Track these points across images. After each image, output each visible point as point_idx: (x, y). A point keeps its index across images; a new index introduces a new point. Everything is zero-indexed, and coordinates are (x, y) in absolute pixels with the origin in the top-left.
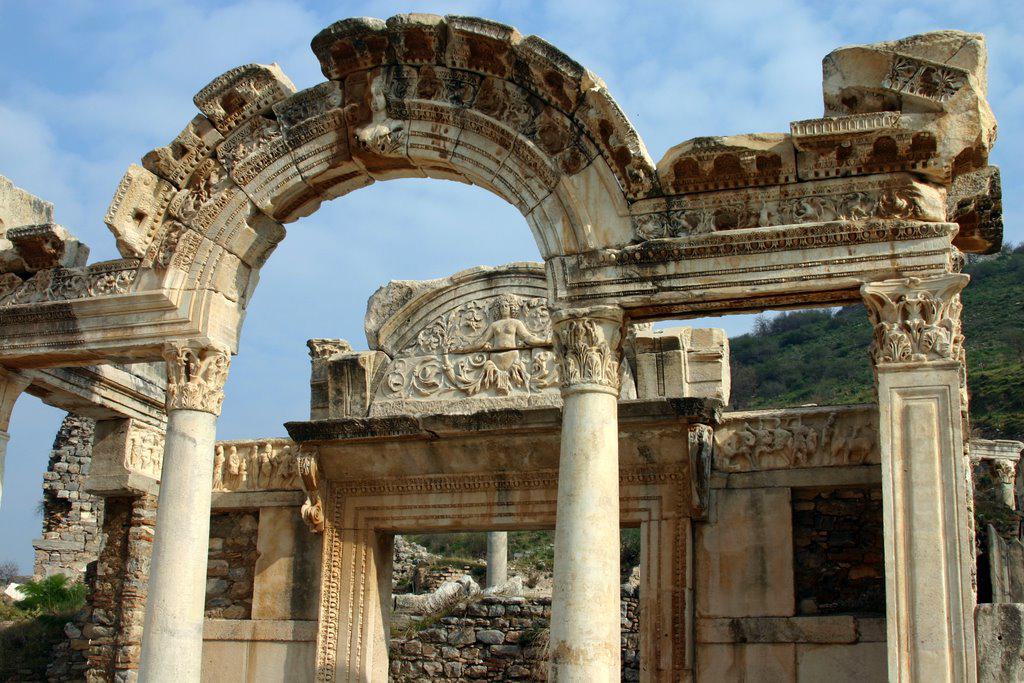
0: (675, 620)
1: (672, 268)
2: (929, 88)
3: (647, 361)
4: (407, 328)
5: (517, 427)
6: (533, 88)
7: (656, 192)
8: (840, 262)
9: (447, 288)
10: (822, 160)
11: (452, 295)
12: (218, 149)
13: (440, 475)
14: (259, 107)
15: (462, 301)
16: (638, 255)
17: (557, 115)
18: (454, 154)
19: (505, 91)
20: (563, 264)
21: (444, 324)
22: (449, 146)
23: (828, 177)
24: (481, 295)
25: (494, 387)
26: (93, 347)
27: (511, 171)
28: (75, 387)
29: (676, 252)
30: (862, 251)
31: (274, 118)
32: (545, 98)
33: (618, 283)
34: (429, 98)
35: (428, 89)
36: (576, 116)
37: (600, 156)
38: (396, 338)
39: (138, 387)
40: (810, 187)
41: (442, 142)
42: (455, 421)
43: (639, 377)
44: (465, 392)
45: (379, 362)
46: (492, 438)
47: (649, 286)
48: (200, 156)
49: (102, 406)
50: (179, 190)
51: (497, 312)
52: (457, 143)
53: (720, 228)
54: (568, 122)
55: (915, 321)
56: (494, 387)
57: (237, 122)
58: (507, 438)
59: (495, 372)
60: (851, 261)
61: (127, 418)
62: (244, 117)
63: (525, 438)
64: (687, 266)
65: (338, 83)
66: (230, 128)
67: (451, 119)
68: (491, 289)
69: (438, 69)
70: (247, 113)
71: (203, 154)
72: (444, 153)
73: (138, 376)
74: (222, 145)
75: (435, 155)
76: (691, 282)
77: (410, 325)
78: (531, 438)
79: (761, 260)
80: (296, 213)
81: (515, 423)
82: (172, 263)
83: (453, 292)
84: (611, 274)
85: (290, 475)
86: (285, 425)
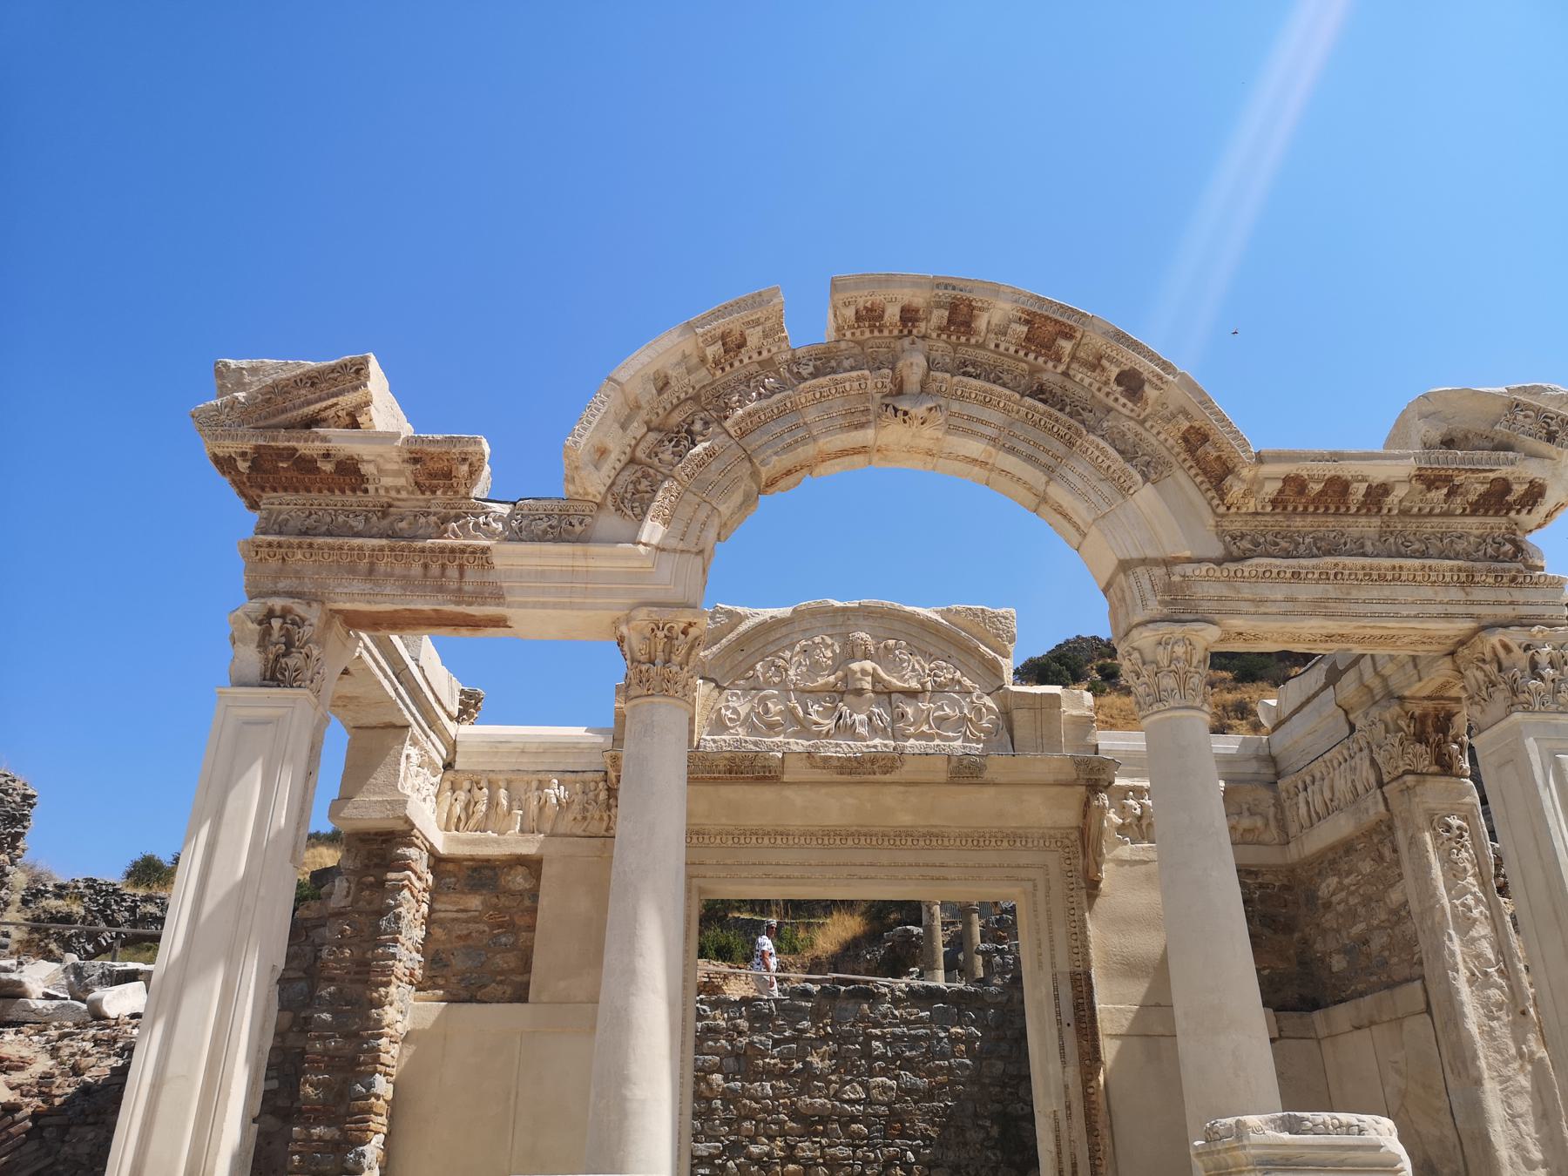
0: (1077, 1007)
2: (1551, 437)
8: (1458, 602)
10: (1433, 494)
23: (1430, 514)
25: (850, 731)
30: (1478, 594)
35: (970, 369)
40: (1412, 525)
44: (818, 735)
51: (851, 652)
55: (1549, 672)
56: (850, 731)
60: (1473, 603)
61: (407, 727)
70: (746, 361)
80: (782, 483)
82: (651, 513)
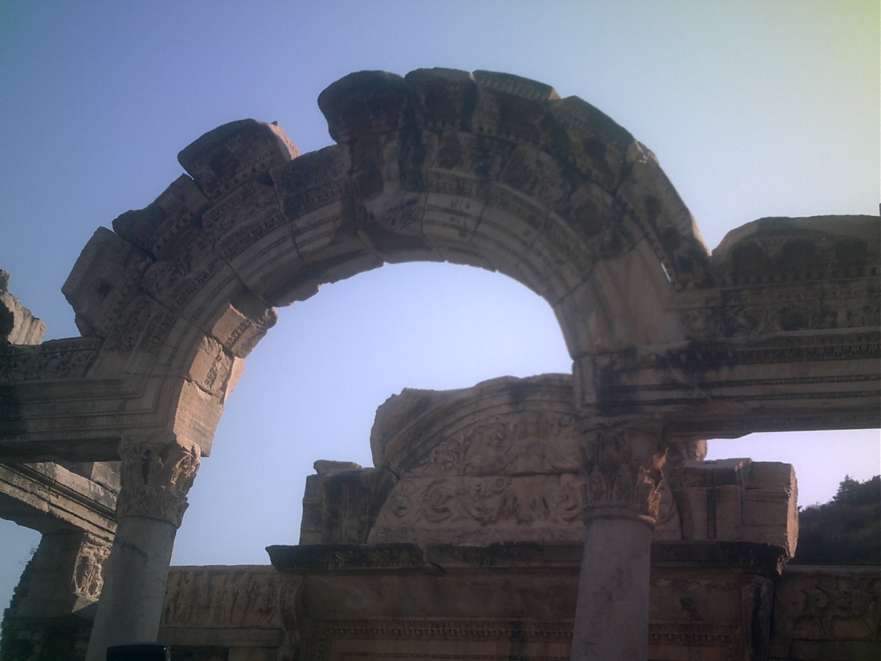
1: (725, 374)
3: (696, 498)
4: (419, 444)
5: (536, 564)
6: (570, 159)
7: (707, 283)
12: (204, 216)
13: (444, 619)
14: (254, 170)
16: (683, 357)
17: (596, 191)
18: (475, 233)
19: (539, 163)
20: (594, 364)
21: (461, 441)
22: (470, 223)
26: (35, 438)
27: (540, 254)
28: (17, 491)
29: (730, 354)
31: (271, 183)
32: (584, 170)
33: (658, 388)
34: (450, 167)
36: (619, 193)
37: (644, 241)
39: (97, 496)
41: (462, 219)
42: (466, 554)
47: (696, 394)
48: (182, 224)
49: (51, 514)
50: (155, 260)
52: (479, 220)
53: (786, 328)
54: (609, 199)
57: (227, 187)
59: (515, 499)
61: (81, 531)
62: (236, 181)
64: (742, 371)
65: (347, 148)
66: (219, 193)
67: (474, 191)
69: (462, 135)
71: (185, 220)
72: (463, 231)
73: (98, 483)
74: (208, 212)
75: (454, 234)
76: (747, 391)
79: (836, 368)
84: (650, 377)
85: (269, 610)
86: (267, 549)
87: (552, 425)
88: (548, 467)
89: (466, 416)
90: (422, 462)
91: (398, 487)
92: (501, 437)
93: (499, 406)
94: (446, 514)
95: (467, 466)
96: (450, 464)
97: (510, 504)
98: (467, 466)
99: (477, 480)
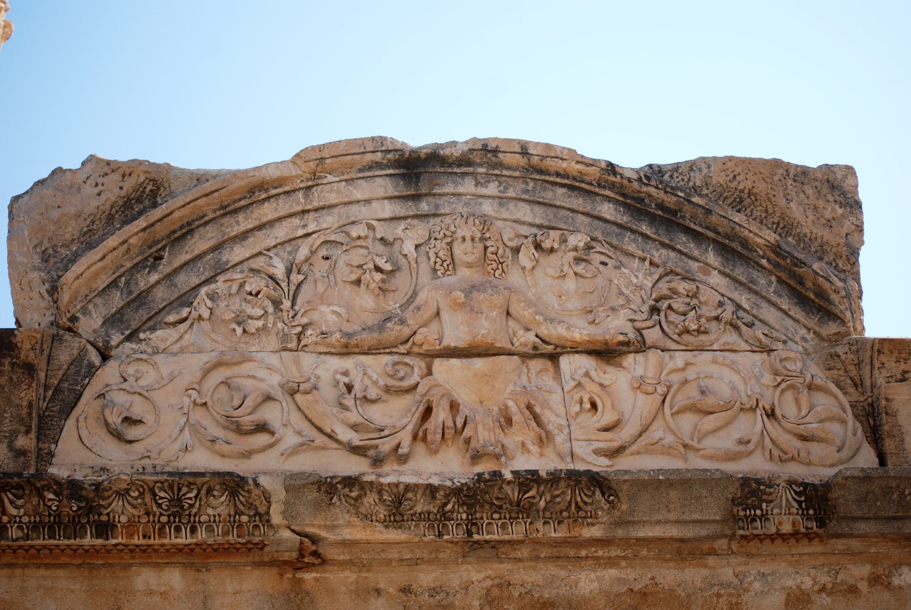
4: (154, 277)
5: (595, 532)
9: (280, 182)
11: (299, 202)
15: (330, 220)
21: (279, 271)
24: (388, 209)
38: (117, 300)
42: (398, 505)
43: (889, 445)
45: (64, 356)
46: (504, 568)
58: (553, 569)
59: (454, 406)
63: (613, 572)
68: (416, 198)
77: (165, 268)
78: (631, 574)
81: (591, 519)
83: (300, 195)
87: (516, 251)
88: (531, 337)
89: (280, 219)
90: (171, 318)
91: (109, 373)
92: (388, 267)
93: (368, 201)
94: (262, 439)
95: (305, 327)
96: (260, 324)
97: (441, 415)
98: (305, 327)
99: (336, 363)
